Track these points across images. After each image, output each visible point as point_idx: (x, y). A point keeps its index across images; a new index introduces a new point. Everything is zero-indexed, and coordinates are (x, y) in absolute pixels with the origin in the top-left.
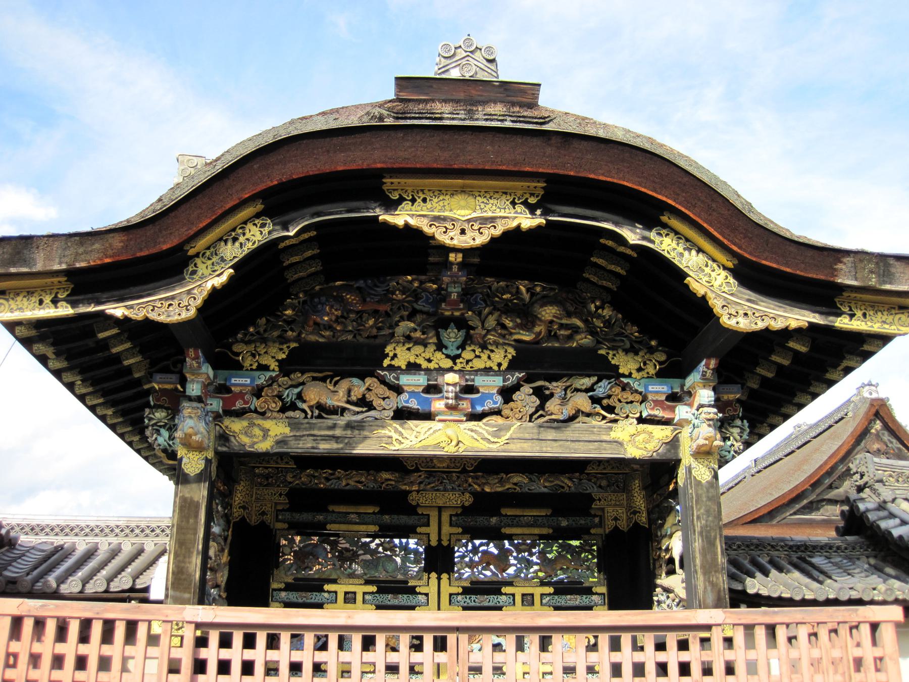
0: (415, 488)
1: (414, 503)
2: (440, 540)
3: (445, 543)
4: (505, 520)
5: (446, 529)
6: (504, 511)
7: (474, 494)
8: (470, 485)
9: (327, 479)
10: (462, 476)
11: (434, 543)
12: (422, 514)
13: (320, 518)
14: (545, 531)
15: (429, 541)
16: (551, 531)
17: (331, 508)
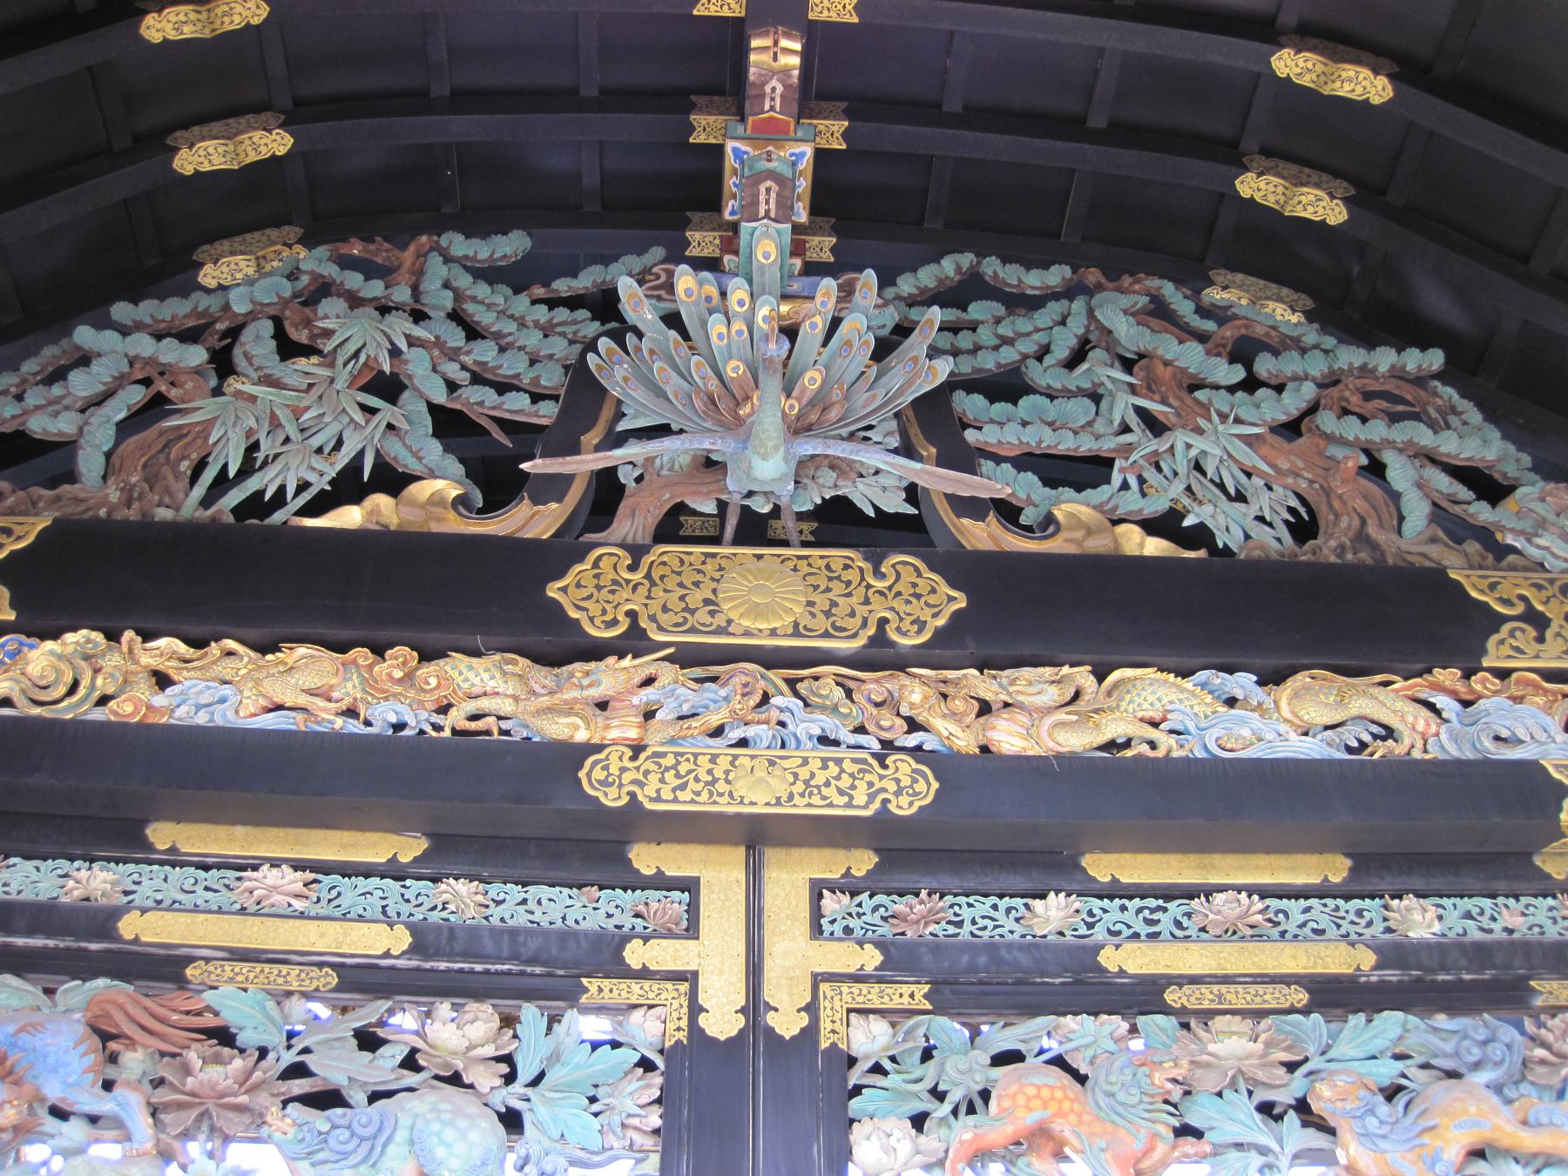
0: (624, 728)
1: (613, 799)
2: (754, 1006)
3: (787, 1024)
4: (1112, 912)
5: (793, 956)
6: (1100, 867)
7: (940, 762)
8: (913, 726)
9: (162, 681)
10: (875, 685)
11: (722, 1023)
12: (661, 883)
13: (96, 881)
14: (1336, 960)
15: (695, 1009)
16: (1367, 959)
17: (161, 834)
